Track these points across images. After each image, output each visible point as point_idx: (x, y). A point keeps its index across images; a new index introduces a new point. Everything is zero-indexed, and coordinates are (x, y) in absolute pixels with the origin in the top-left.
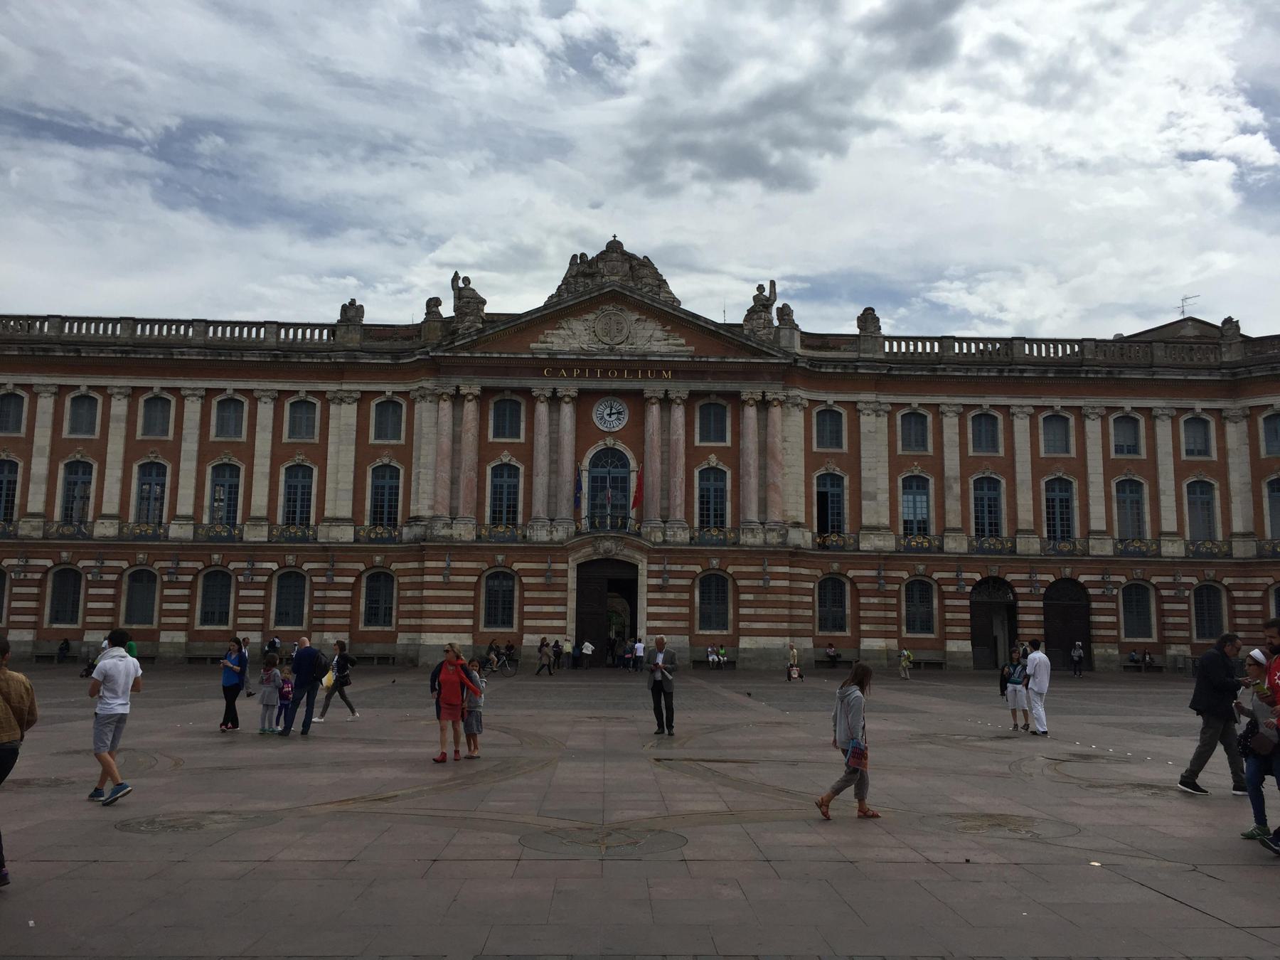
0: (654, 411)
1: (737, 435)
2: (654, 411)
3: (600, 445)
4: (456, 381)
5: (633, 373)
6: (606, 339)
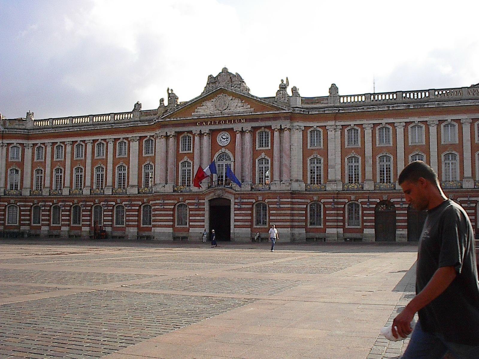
0: (238, 136)
3: (220, 152)
4: (166, 130)
5: (230, 121)
6: (220, 109)
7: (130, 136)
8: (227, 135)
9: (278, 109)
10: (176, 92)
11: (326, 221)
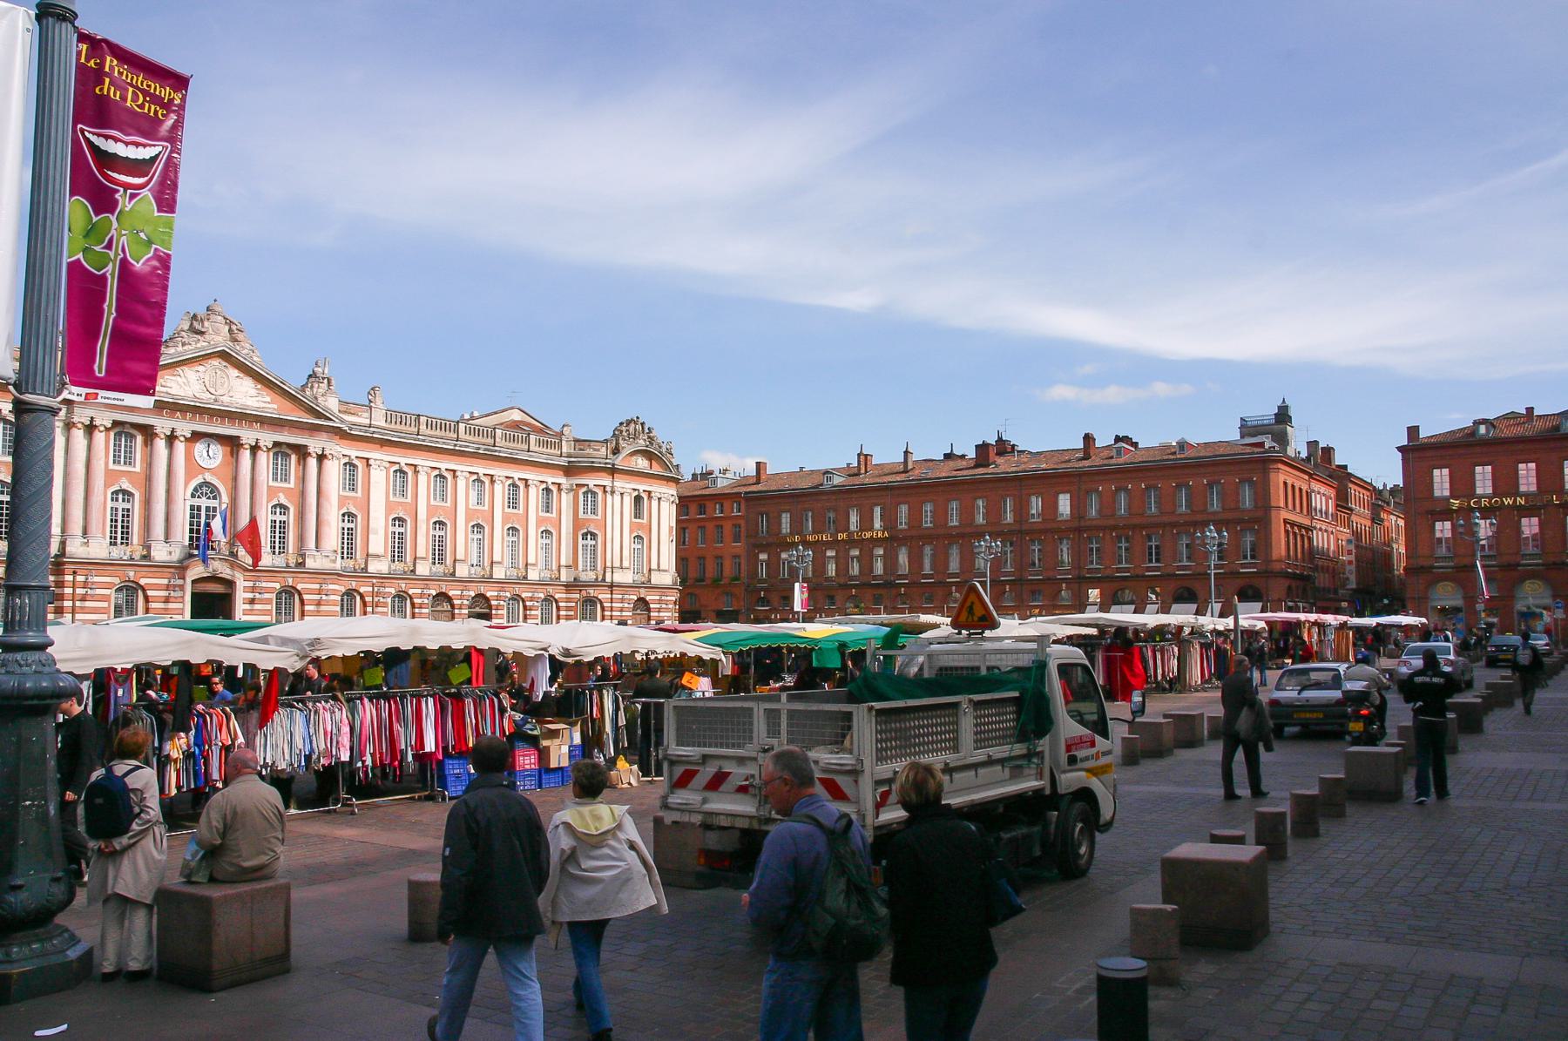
1: (303, 479)
2: (246, 455)
3: (199, 480)
8: (218, 451)
9: (319, 415)
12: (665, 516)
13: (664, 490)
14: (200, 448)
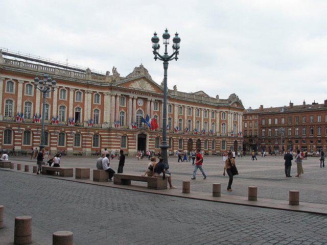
7: (86, 89)
10: (118, 71)
11: (173, 146)
12: (240, 119)
13: (241, 112)
14: (139, 101)
